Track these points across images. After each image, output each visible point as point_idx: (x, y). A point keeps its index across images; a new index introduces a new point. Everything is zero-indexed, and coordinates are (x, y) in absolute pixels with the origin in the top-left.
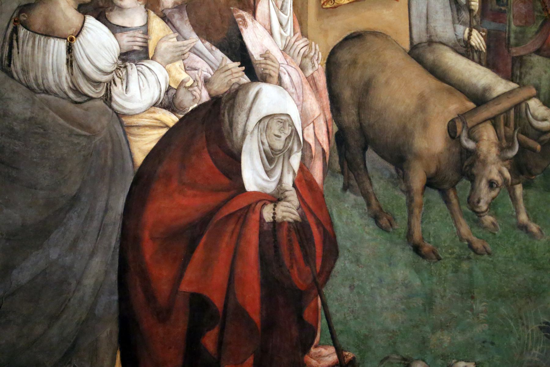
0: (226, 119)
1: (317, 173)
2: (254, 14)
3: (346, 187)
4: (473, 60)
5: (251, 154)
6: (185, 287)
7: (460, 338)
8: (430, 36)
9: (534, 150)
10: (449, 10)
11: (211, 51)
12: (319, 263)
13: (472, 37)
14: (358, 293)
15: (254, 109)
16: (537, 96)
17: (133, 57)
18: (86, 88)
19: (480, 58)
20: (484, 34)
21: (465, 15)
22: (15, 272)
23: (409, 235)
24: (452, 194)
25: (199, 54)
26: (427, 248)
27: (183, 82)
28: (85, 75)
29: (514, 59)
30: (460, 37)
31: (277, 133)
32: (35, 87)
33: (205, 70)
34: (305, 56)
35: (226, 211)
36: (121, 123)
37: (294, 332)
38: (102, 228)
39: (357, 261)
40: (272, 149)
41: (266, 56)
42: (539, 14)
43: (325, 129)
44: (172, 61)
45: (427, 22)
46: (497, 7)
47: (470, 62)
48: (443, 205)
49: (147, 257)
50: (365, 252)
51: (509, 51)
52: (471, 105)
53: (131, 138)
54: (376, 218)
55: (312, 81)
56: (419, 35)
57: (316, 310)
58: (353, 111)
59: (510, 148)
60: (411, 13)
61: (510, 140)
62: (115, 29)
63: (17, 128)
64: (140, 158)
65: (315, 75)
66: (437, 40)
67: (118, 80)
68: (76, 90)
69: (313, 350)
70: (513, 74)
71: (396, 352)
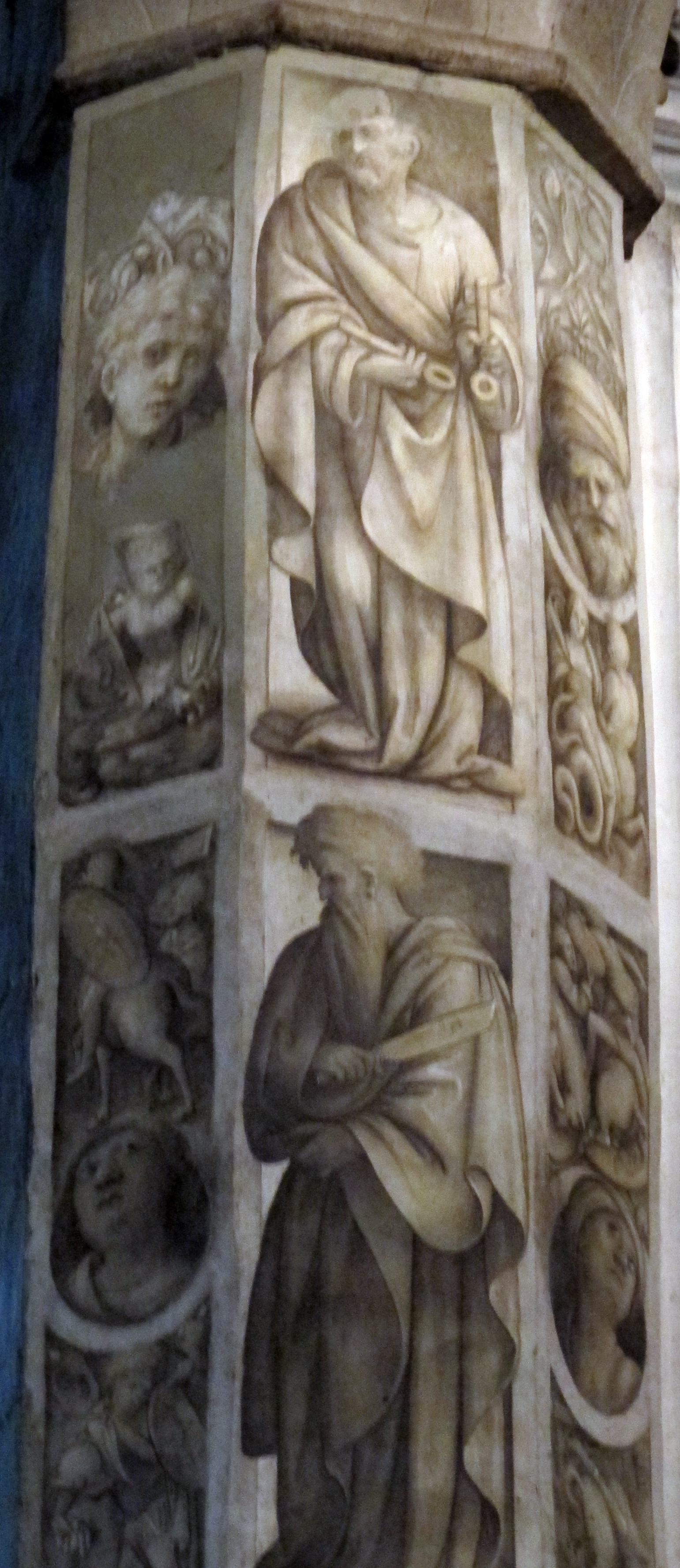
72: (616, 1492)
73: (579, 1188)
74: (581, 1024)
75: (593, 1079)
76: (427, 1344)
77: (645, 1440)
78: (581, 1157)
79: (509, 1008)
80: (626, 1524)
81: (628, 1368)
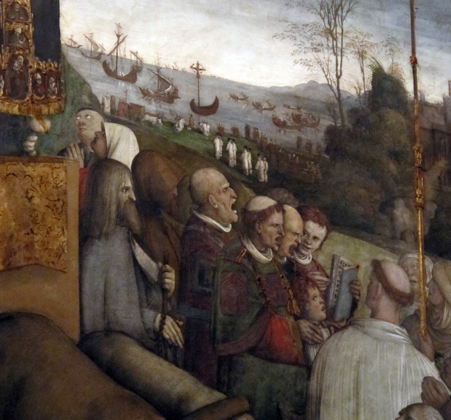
4: (166, 358)
8: (109, 323)
10: (134, 288)
13: (165, 327)
19: (175, 355)
20: (181, 323)
21: (157, 297)
29: (221, 360)
30: (149, 325)
42: (254, 300)
46: (200, 288)
47: (162, 361)
51: (214, 349)
60: (83, 289)
66: (118, 329)
70: (219, 381)
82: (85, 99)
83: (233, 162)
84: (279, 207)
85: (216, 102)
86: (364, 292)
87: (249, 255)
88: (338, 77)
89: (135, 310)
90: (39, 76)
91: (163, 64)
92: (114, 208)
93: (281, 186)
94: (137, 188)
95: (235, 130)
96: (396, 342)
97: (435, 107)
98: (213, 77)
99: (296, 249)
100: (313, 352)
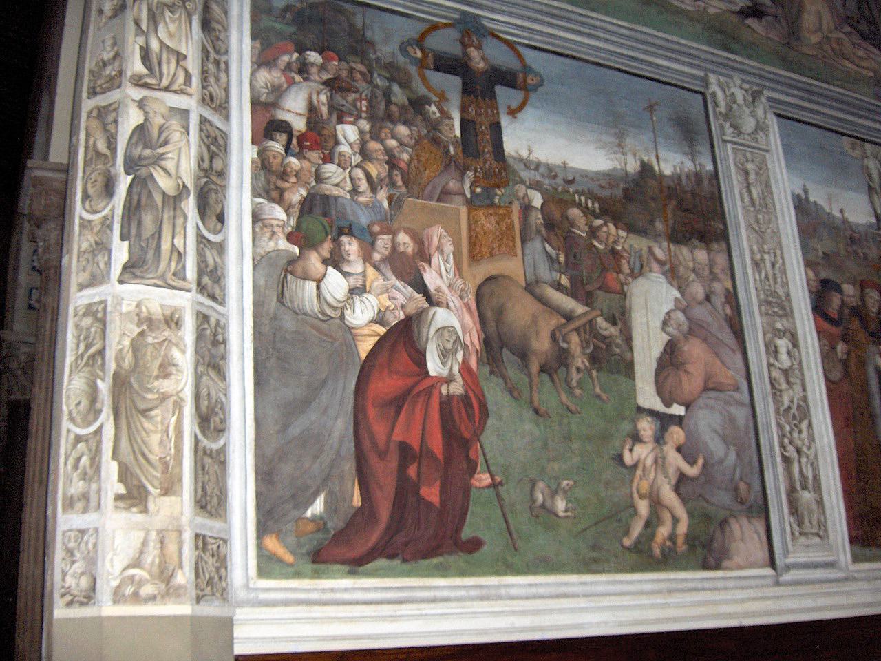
0: (416, 330)
1: (473, 363)
2: (430, 264)
3: (492, 373)
4: (563, 293)
5: (432, 352)
6: (397, 437)
7: (564, 466)
9: (602, 349)
11: (404, 287)
12: (477, 421)
14: (503, 440)
15: (433, 323)
16: (602, 315)
17: (357, 291)
18: (329, 311)
21: (556, 266)
22: (290, 428)
23: (531, 402)
24: (555, 377)
25: (398, 290)
26: (542, 409)
27: (388, 307)
28: (328, 304)
29: (586, 293)
31: (447, 338)
32: (298, 311)
33: (401, 299)
34: (462, 290)
35: (418, 389)
36: (352, 334)
37: (464, 465)
38: (342, 401)
39: (501, 419)
40: (445, 348)
41: (438, 290)
43: (476, 336)
44: (381, 294)
45: (535, 270)
48: (550, 383)
49: (371, 417)
50: (506, 413)
52: (563, 321)
53: (357, 343)
54: (511, 392)
55: (467, 306)
56: (530, 278)
57: (477, 452)
58: (493, 324)
59: (588, 347)
61: (588, 342)
62: (346, 275)
63: (288, 337)
64: (363, 355)
65: (469, 302)
67: (348, 306)
68: (323, 313)
69: (476, 476)
71: (527, 476)
72: (215, 252)
73: (206, 183)
74: (208, 147)
75: (211, 161)
76: (166, 216)
77: (224, 241)
78: (206, 176)
79: (188, 141)
80: (218, 259)
81: (219, 225)
82: (518, 179)
83: (583, 205)
84: (606, 224)
85: (574, 179)
86: (645, 261)
87: (595, 246)
88: (626, 165)
89: (548, 272)
90: (497, 170)
91: (549, 162)
92: (534, 228)
93: (606, 215)
94: (544, 218)
95: (583, 190)
96: (661, 282)
97: (668, 176)
98: (572, 168)
99: (614, 242)
100: (626, 288)
